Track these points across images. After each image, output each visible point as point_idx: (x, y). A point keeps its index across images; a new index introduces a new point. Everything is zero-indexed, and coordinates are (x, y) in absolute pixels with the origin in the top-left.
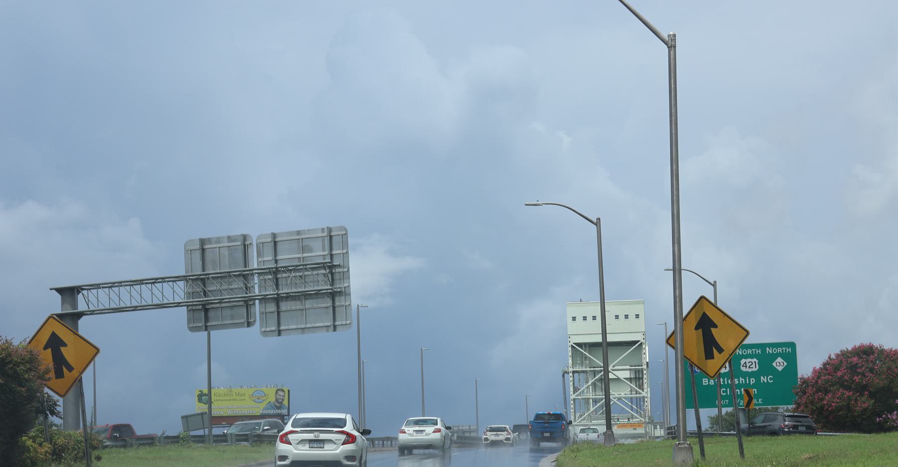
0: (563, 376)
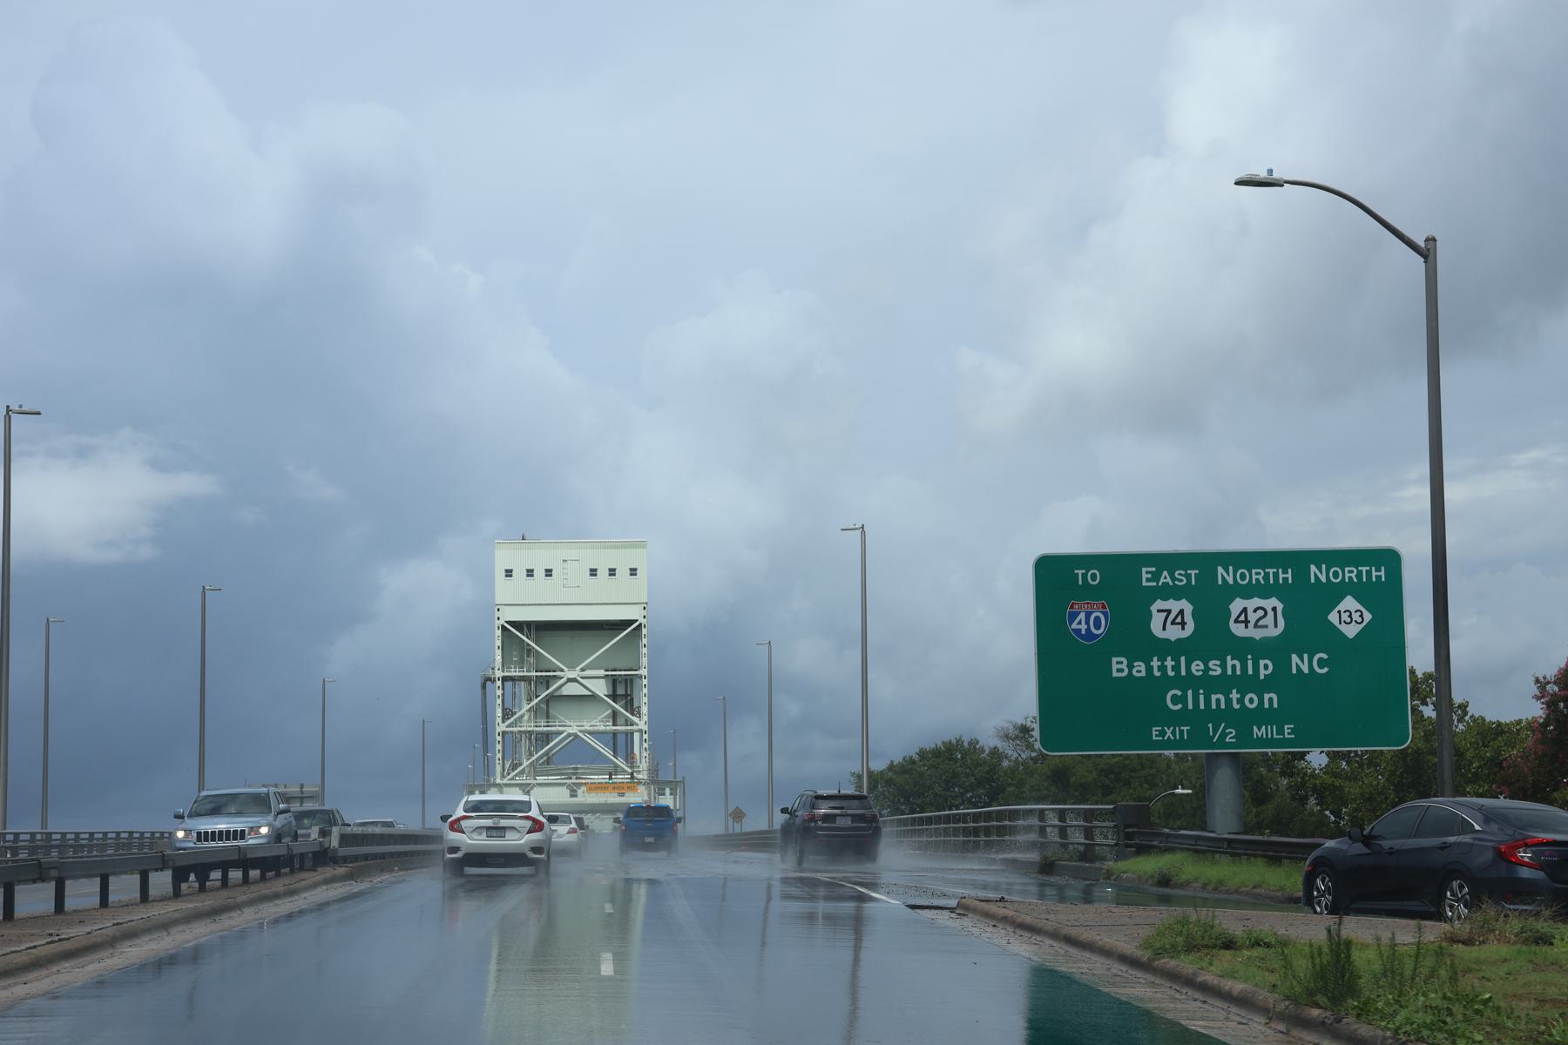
0: (484, 686)
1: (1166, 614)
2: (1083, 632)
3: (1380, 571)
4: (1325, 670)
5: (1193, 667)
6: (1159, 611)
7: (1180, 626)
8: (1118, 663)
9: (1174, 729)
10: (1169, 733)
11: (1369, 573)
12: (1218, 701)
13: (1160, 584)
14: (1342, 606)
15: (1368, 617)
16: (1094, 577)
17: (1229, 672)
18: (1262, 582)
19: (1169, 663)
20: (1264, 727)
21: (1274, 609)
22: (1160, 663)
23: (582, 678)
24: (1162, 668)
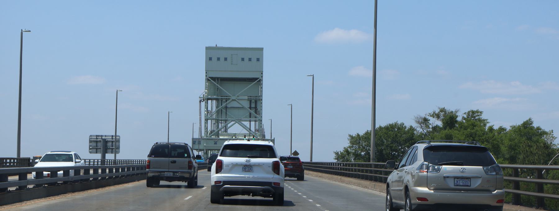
0: (200, 101)
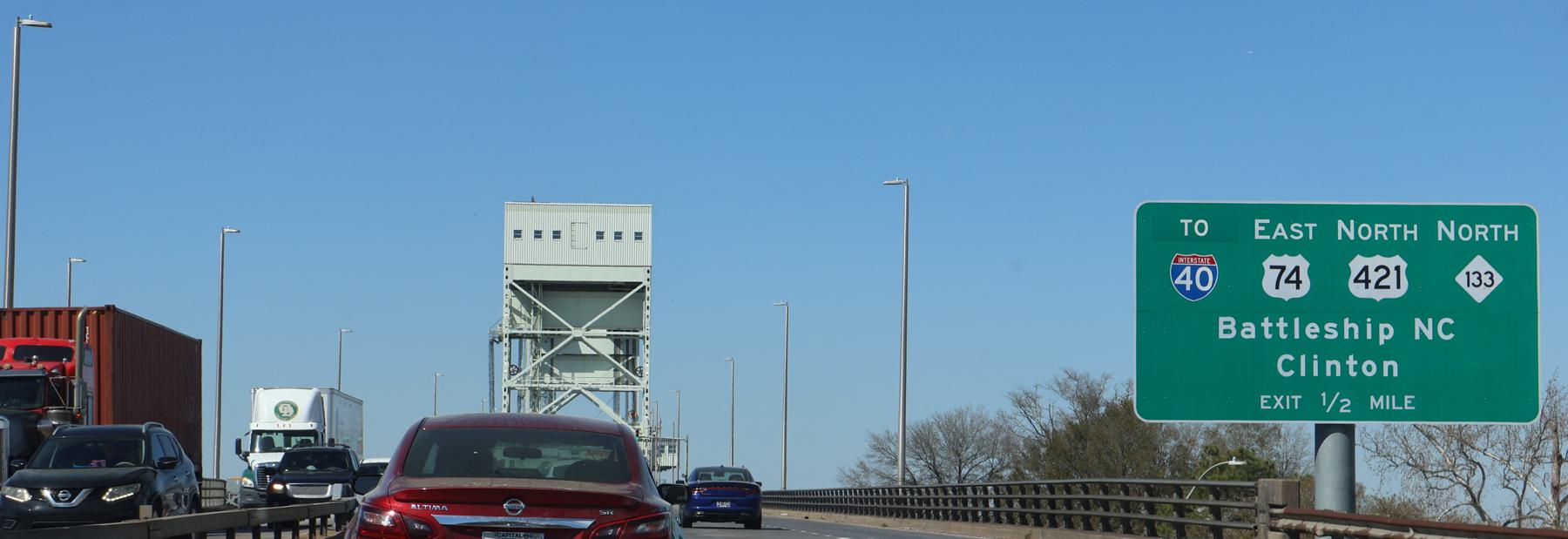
0: (491, 343)
1: (1279, 271)
2: (1188, 288)
3: (1513, 230)
4: (1451, 336)
5: (1308, 331)
6: (1272, 267)
7: (1295, 285)
8: (1225, 323)
9: (1285, 398)
10: (1279, 401)
11: (1501, 231)
12: (1333, 367)
13: (1274, 238)
14: (1471, 267)
15: (1498, 279)
16: (1202, 229)
17: (1346, 336)
18: (1386, 238)
19: (1282, 324)
20: (1382, 397)
21: (1398, 268)
22: (1271, 325)
23: (587, 337)
24: (1274, 330)
